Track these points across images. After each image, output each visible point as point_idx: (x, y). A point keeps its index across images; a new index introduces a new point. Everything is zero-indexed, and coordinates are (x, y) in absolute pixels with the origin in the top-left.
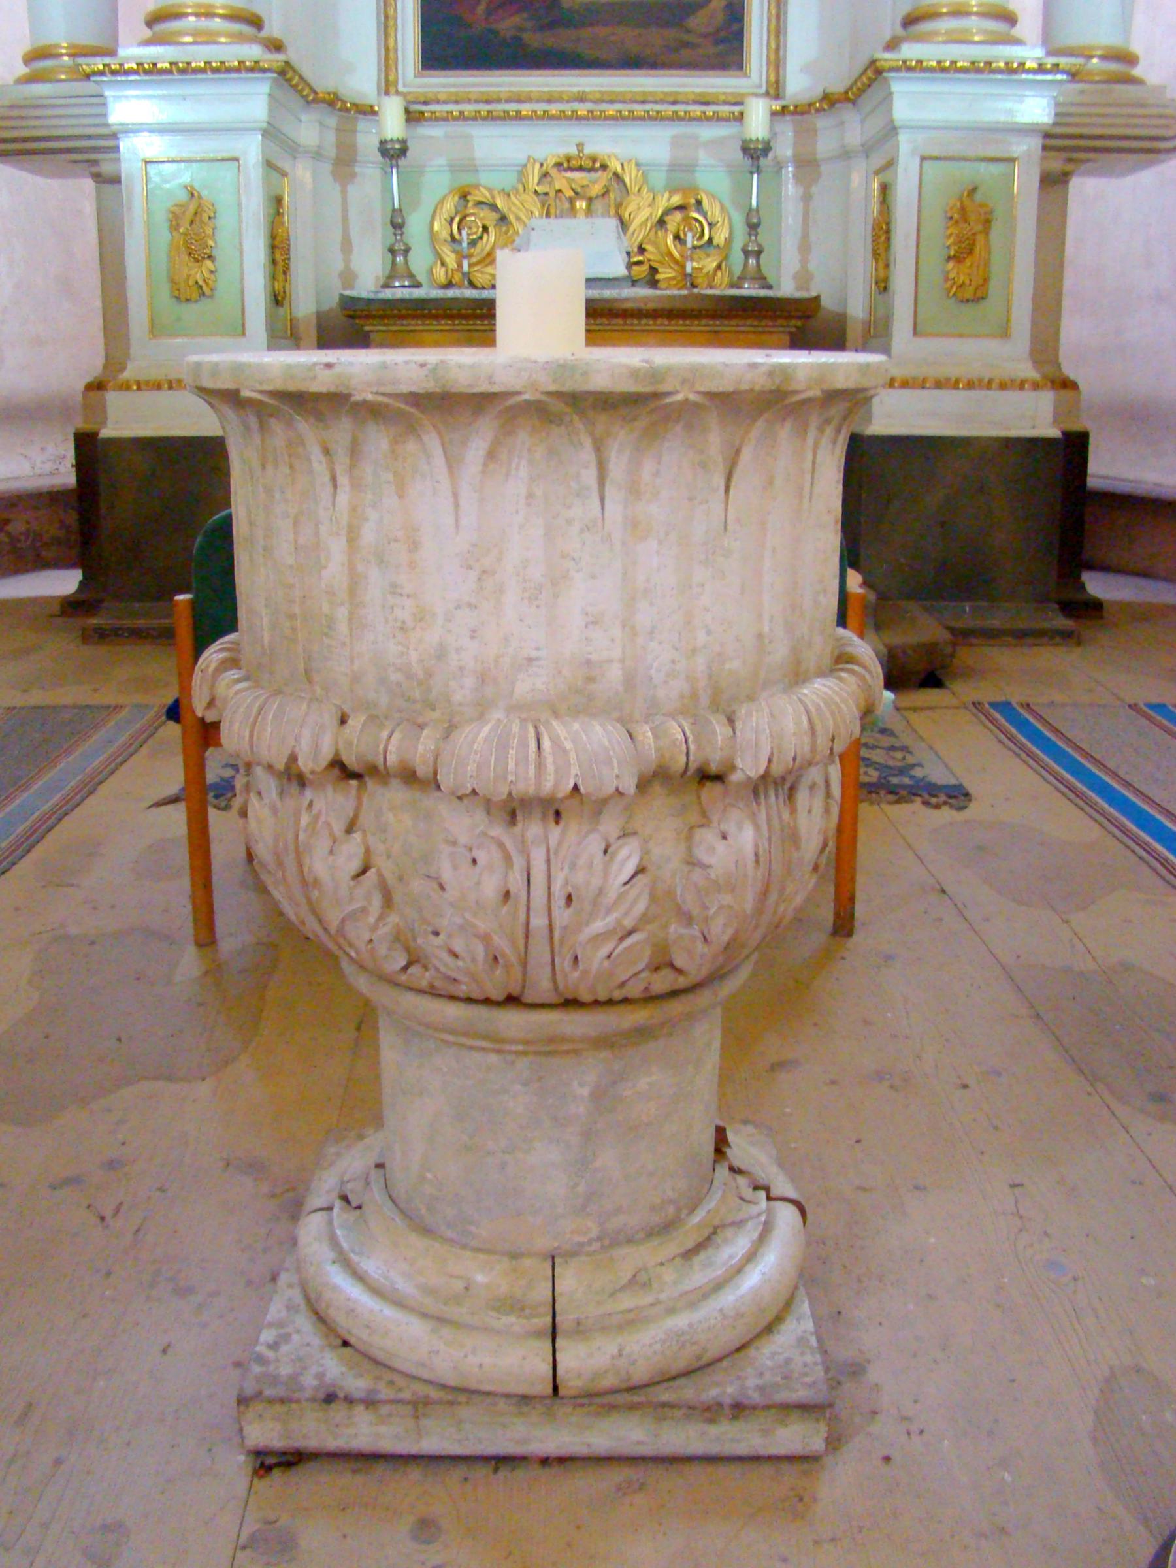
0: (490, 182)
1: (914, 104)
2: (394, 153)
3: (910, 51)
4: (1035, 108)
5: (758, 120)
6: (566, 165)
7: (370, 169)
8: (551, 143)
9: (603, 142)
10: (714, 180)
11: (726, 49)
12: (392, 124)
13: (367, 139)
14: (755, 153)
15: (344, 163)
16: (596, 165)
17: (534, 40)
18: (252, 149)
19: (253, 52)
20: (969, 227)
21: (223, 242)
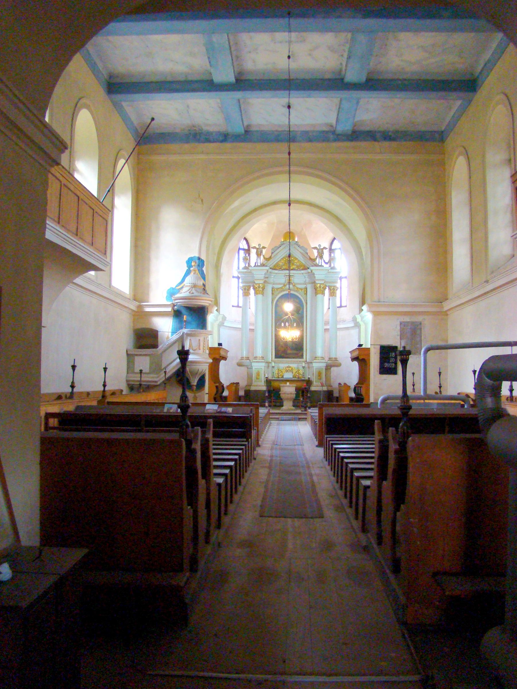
0: (281, 368)
1: (315, 365)
2: (273, 367)
3: (315, 361)
4: (325, 365)
5: (304, 364)
6: (288, 367)
7: (270, 368)
8: (287, 365)
9: (291, 365)
10: (301, 368)
11: (302, 357)
12: (273, 364)
13: (270, 365)
14: (303, 367)
15: (268, 366)
16: (290, 367)
17: (285, 356)
18: (263, 368)
19: (263, 361)
20: (320, 374)
21: (260, 374)
